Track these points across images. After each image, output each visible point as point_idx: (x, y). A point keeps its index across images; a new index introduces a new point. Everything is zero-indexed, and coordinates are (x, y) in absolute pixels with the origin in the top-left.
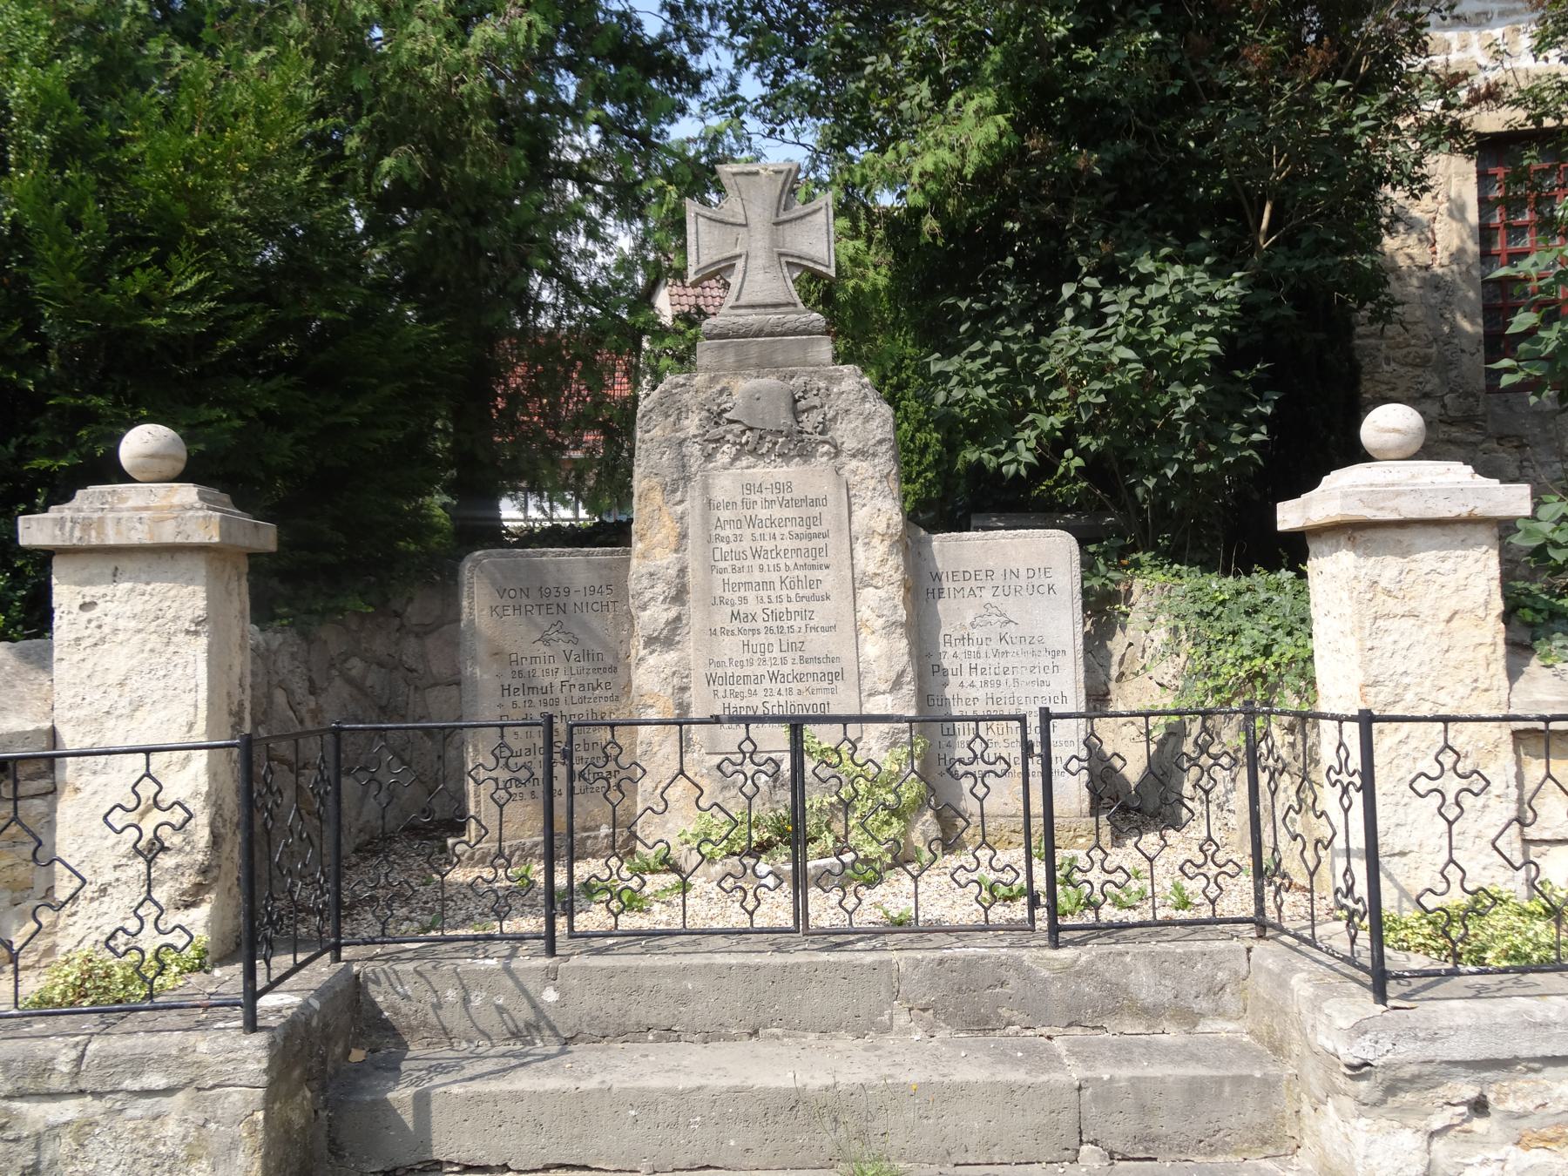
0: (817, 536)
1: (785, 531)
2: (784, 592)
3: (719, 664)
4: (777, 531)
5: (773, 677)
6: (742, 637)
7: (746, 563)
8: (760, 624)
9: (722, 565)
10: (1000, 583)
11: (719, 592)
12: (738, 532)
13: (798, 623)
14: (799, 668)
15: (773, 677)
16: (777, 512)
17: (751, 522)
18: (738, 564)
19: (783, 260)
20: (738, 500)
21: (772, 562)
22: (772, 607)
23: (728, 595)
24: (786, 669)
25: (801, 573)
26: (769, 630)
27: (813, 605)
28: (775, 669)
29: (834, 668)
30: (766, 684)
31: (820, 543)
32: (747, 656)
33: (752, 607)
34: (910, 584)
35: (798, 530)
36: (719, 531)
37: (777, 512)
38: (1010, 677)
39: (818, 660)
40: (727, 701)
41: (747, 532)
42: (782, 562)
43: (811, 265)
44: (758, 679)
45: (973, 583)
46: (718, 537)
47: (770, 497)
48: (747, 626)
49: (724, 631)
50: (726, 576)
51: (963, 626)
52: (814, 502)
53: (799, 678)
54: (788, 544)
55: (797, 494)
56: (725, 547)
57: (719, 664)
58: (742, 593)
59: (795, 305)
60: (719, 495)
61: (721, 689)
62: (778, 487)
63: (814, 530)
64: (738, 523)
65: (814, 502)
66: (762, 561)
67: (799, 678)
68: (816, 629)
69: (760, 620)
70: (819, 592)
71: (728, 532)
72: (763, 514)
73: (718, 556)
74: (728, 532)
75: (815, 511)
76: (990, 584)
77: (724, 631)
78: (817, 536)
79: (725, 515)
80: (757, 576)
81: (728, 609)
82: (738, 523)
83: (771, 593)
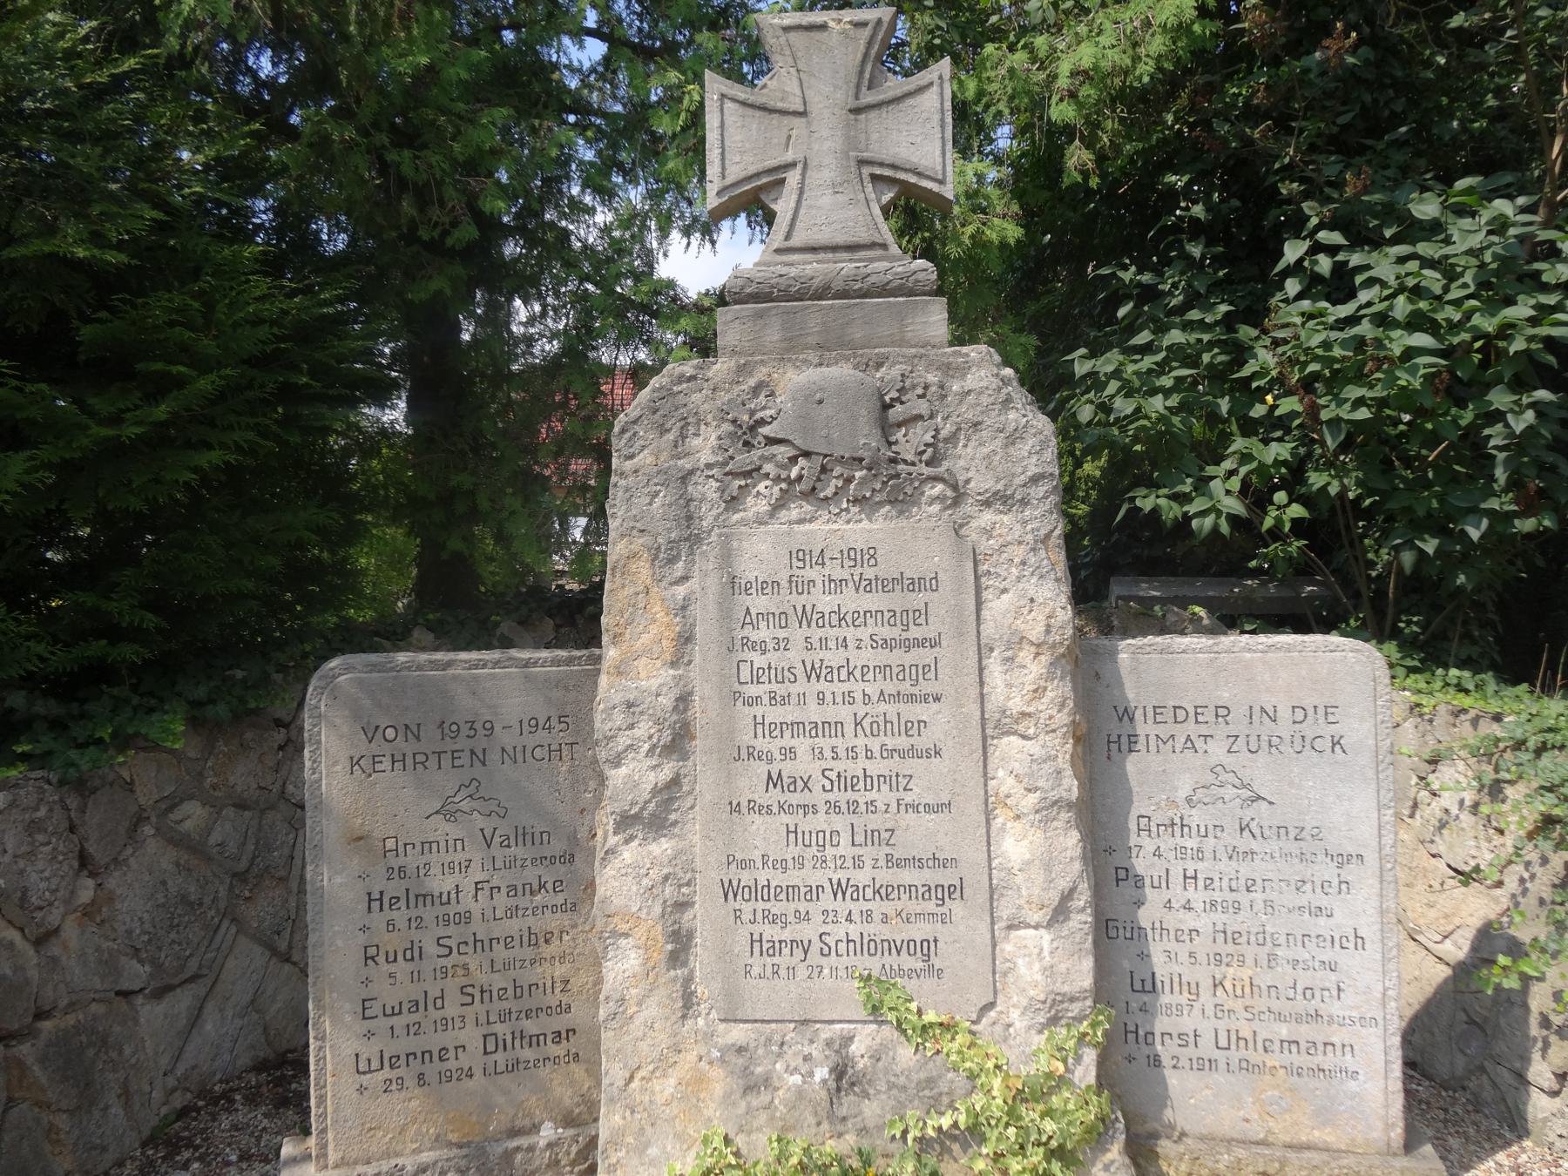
0: (920, 643)
1: (863, 634)
2: (861, 741)
3: (745, 864)
4: (850, 633)
5: (839, 890)
6: (785, 818)
7: (795, 689)
8: (817, 797)
9: (752, 690)
10: (1241, 728)
11: (746, 738)
12: (782, 634)
13: (883, 796)
14: (885, 876)
15: (839, 890)
16: (851, 601)
17: (805, 617)
18: (781, 690)
19: (866, 171)
20: (783, 577)
21: (840, 688)
22: (839, 766)
23: (761, 744)
24: (862, 877)
25: (891, 709)
26: (834, 807)
27: (912, 766)
28: (841, 875)
29: (947, 877)
30: (827, 901)
31: (924, 656)
32: (794, 851)
33: (803, 765)
34: (1084, 728)
35: (886, 632)
36: (748, 631)
37: (851, 601)
38: (1258, 896)
39: (918, 863)
40: (757, 929)
41: (797, 634)
42: (857, 688)
43: (913, 179)
44: (814, 892)
45: (1191, 728)
46: (746, 643)
47: (838, 574)
48: (795, 799)
49: (753, 806)
50: (758, 711)
51: (1172, 803)
52: (915, 585)
53: (884, 893)
54: (868, 656)
55: (886, 569)
56: (759, 661)
57: (745, 864)
58: (787, 741)
59: (884, 246)
60: (749, 570)
61: (747, 908)
62: (852, 556)
63: (915, 633)
64: (782, 619)
65: (915, 585)
66: (823, 685)
67: (884, 893)
68: (915, 807)
69: (817, 788)
70: (922, 742)
71: (763, 633)
72: (826, 603)
73: (745, 674)
74: (763, 633)
75: (917, 599)
76: (1221, 731)
77: (753, 806)
78: (920, 643)
79: (759, 603)
80: (814, 713)
81: (762, 769)
82: (782, 619)
83: (838, 742)
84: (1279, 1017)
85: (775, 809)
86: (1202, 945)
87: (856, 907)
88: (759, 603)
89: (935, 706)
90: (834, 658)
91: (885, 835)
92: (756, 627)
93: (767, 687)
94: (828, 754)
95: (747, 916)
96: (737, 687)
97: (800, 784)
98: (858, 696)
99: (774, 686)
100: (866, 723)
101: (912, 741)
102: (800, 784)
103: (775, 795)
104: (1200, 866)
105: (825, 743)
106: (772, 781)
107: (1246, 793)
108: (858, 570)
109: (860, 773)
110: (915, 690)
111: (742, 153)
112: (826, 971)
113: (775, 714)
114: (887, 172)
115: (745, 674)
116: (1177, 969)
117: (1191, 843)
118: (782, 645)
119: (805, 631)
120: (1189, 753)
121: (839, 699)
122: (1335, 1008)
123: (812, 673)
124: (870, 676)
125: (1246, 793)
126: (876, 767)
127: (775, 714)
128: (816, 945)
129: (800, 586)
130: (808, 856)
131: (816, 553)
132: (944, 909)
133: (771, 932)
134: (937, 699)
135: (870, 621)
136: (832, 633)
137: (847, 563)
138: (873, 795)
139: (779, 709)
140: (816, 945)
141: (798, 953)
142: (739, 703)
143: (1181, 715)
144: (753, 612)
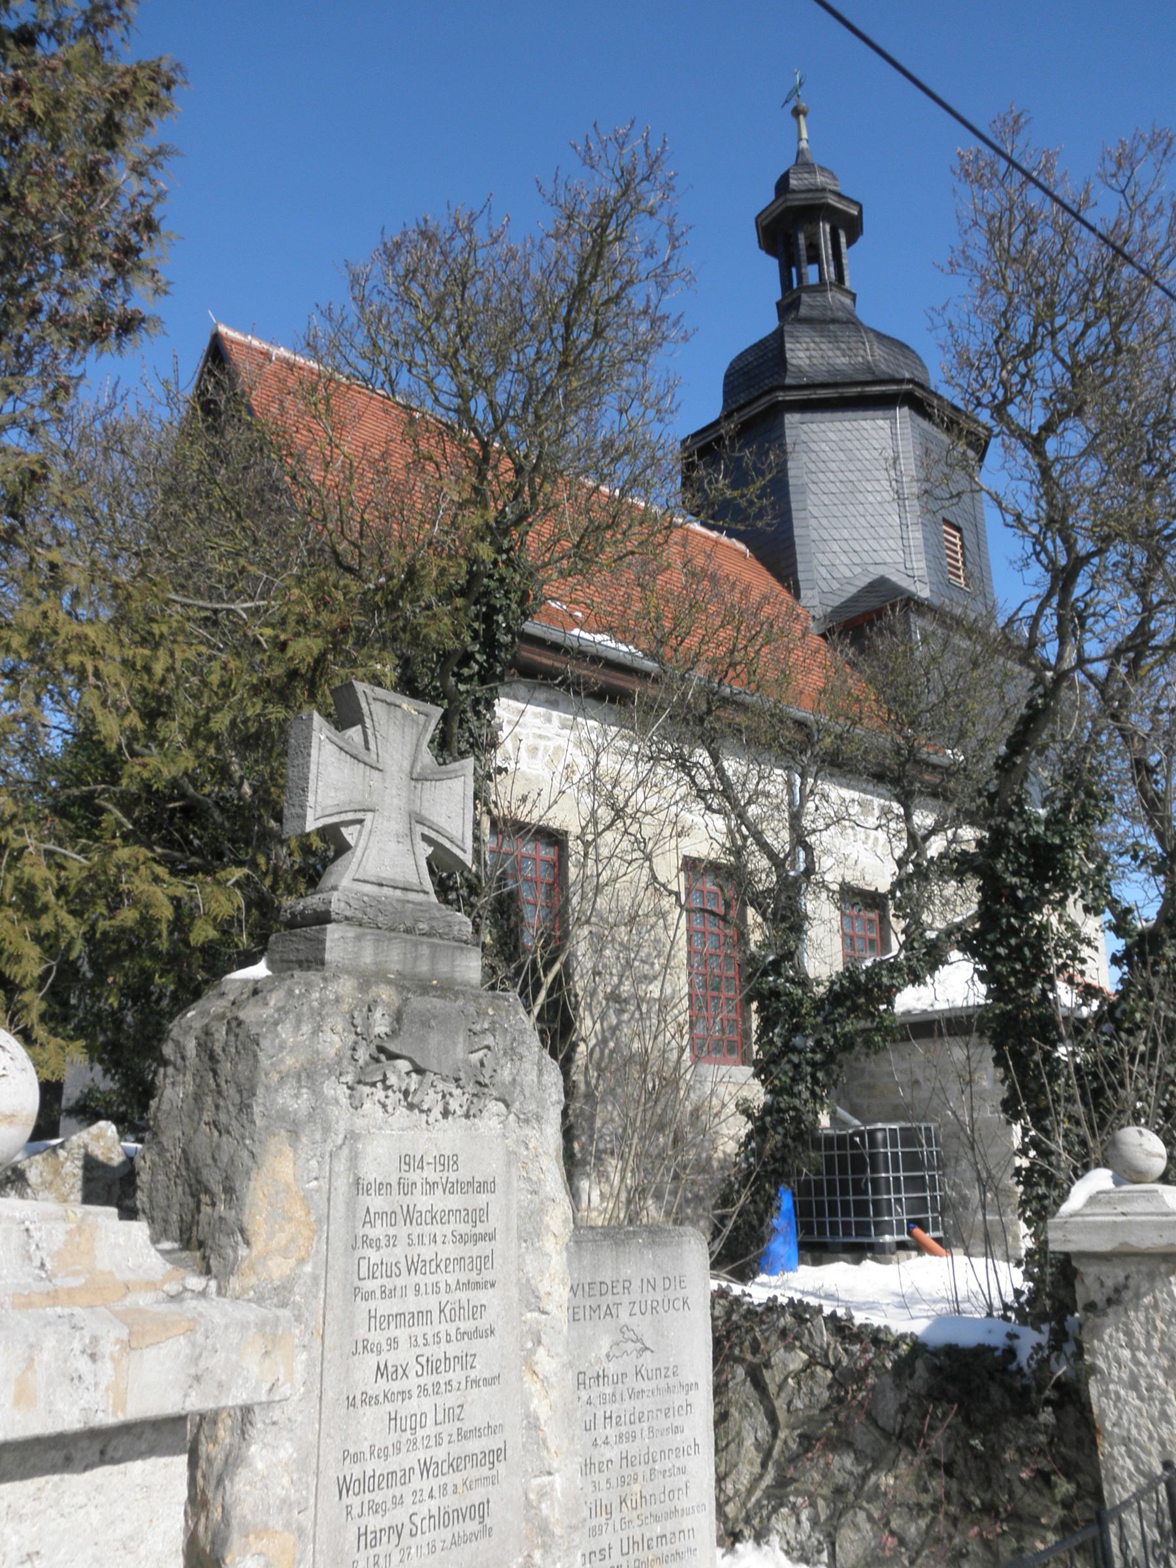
0: (483, 1237)
1: (447, 1229)
2: (443, 1327)
3: (356, 1458)
4: (438, 1229)
5: (425, 1468)
6: (389, 1407)
7: (400, 1282)
8: (412, 1383)
9: (370, 1285)
10: (636, 1295)
11: (362, 1333)
12: (392, 1231)
13: (457, 1375)
14: (457, 1449)
15: (425, 1468)
16: (442, 1201)
17: (409, 1216)
18: (389, 1283)
19: (419, 829)
20: (394, 1181)
21: (430, 1279)
22: (427, 1351)
23: (376, 1337)
24: (440, 1454)
25: (463, 1295)
26: (423, 1390)
27: (477, 1345)
28: (422, 1455)
29: (494, 1443)
30: (416, 1482)
31: (484, 1248)
32: (394, 1437)
33: (403, 1356)
35: (464, 1228)
36: (368, 1230)
37: (442, 1201)
38: (645, 1425)
39: (476, 1432)
40: (362, 1522)
41: (402, 1230)
42: (441, 1277)
43: (448, 844)
44: (406, 1476)
45: (609, 1299)
46: (367, 1241)
47: (433, 1177)
48: (396, 1386)
49: (369, 1400)
50: (372, 1304)
51: (598, 1360)
52: (484, 1187)
53: (454, 1466)
54: (450, 1250)
55: (463, 1175)
56: (374, 1256)
57: (356, 1458)
58: (393, 1332)
59: (426, 893)
60: (370, 1173)
61: (355, 1501)
62: (448, 1162)
63: (480, 1229)
64: (390, 1217)
65: (484, 1187)
66: (419, 1278)
67: (454, 1466)
68: (476, 1382)
69: (412, 1374)
70: (483, 1324)
71: (378, 1231)
72: (423, 1202)
73: (364, 1272)
74: (378, 1231)
75: (482, 1199)
76: (626, 1299)
77: (369, 1400)
78: (483, 1237)
79: (376, 1203)
80: (412, 1304)
81: (372, 1360)
82: (390, 1217)
83: (428, 1329)
84: (657, 1519)
85: (381, 1399)
86: (613, 1473)
87: (435, 1483)
88: (376, 1203)
89: (491, 1291)
90: (427, 1252)
91: (457, 1411)
92: (373, 1226)
93: (379, 1282)
94: (421, 1341)
95: (356, 1511)
96: (357, 1283)
97: (400, 1371)
98: (442, 1286)
99: (385, 1281)
100: (447, 1311)
101: (476, 1323)
102: (400, 1371)
103: (383, 1385)
104: (615, 1407)
105: (418, 1330)
106: (381, 1371)
107: (639, 1345)
108: (446, 1174)
109: (442, 1357)
110: (478, 1278)
111: (336, 790)
112: (413, 1551)
113: (385, 1307)
114: (433, 835)
115: (364, 1272)
116: (599, 1495)
117: (608, 1390)
118: (392, 1241)
119: (407, 1229)
120: (608, 1318)
121: (429, 1290)
122: (683, 1503)
123: (412, 1267)
124: (450, 1268)
125: (639, 1345)
126: (453, 1349)
127: (385, 1307)
128: (408, 1526)
129: (406, 1188)
130: (404, 1441)
131: (418, 1159)
132: (494, 1472)
133: (375, 1522)
134: (493, 1285)
135: (452, 1219)
136: (427, 1229)
137: (439, 1168)
138: (450, 1375)
139: (388, 1301)
140: (408, 1526)
141: (394, 1538)
142: (358, 1298)
143: (604, 1287)
144: (372, 1211)
